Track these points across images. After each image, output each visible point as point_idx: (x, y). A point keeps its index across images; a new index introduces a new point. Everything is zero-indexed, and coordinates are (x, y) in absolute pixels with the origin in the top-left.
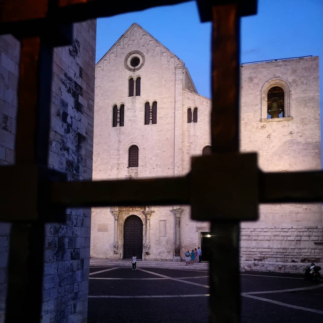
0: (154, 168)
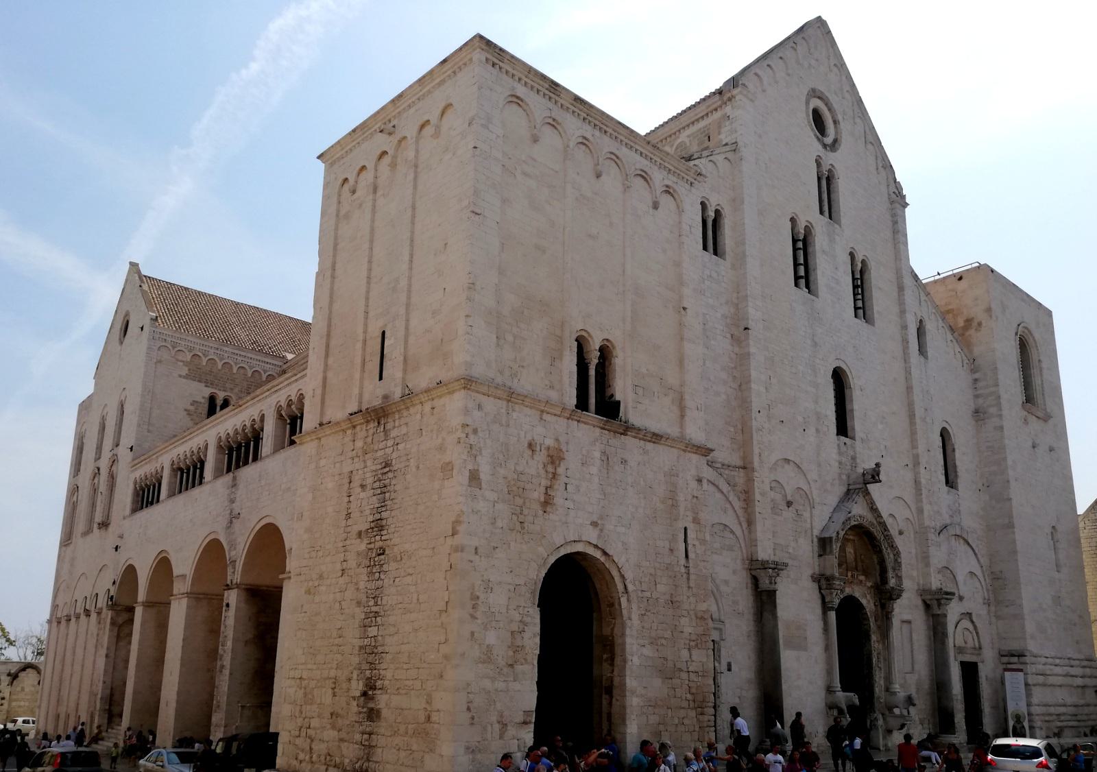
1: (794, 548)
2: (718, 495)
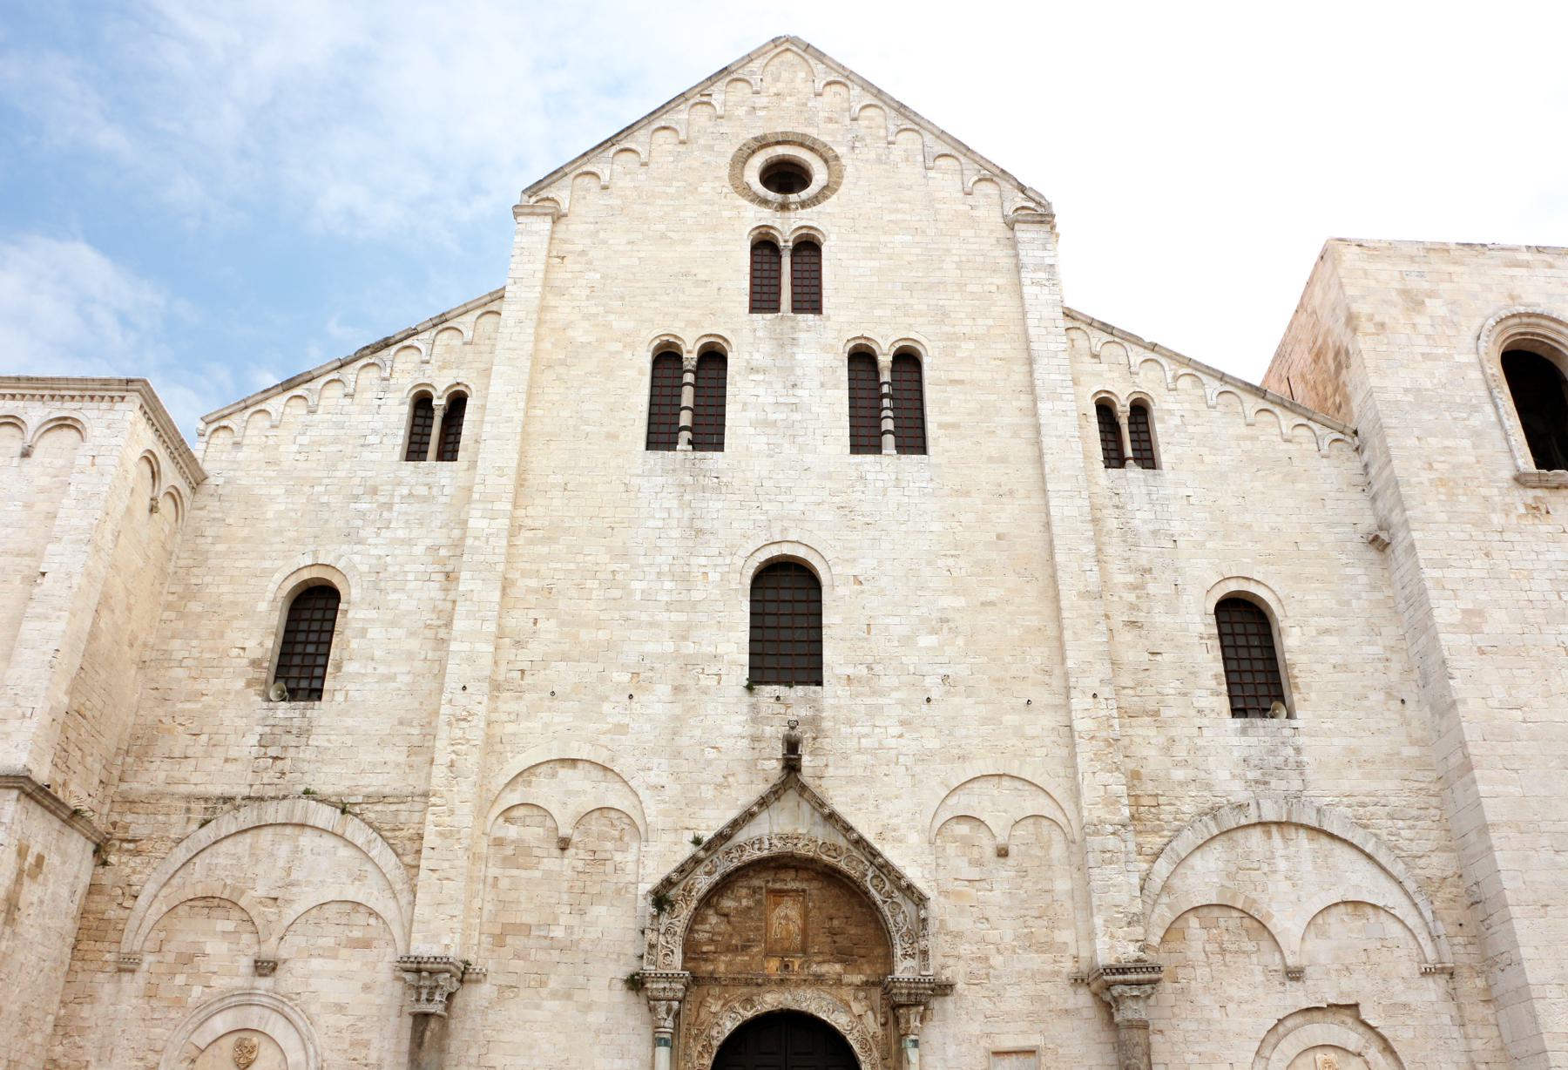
0: (928, 700)
1: (569, 928)
2: (344, 852)
